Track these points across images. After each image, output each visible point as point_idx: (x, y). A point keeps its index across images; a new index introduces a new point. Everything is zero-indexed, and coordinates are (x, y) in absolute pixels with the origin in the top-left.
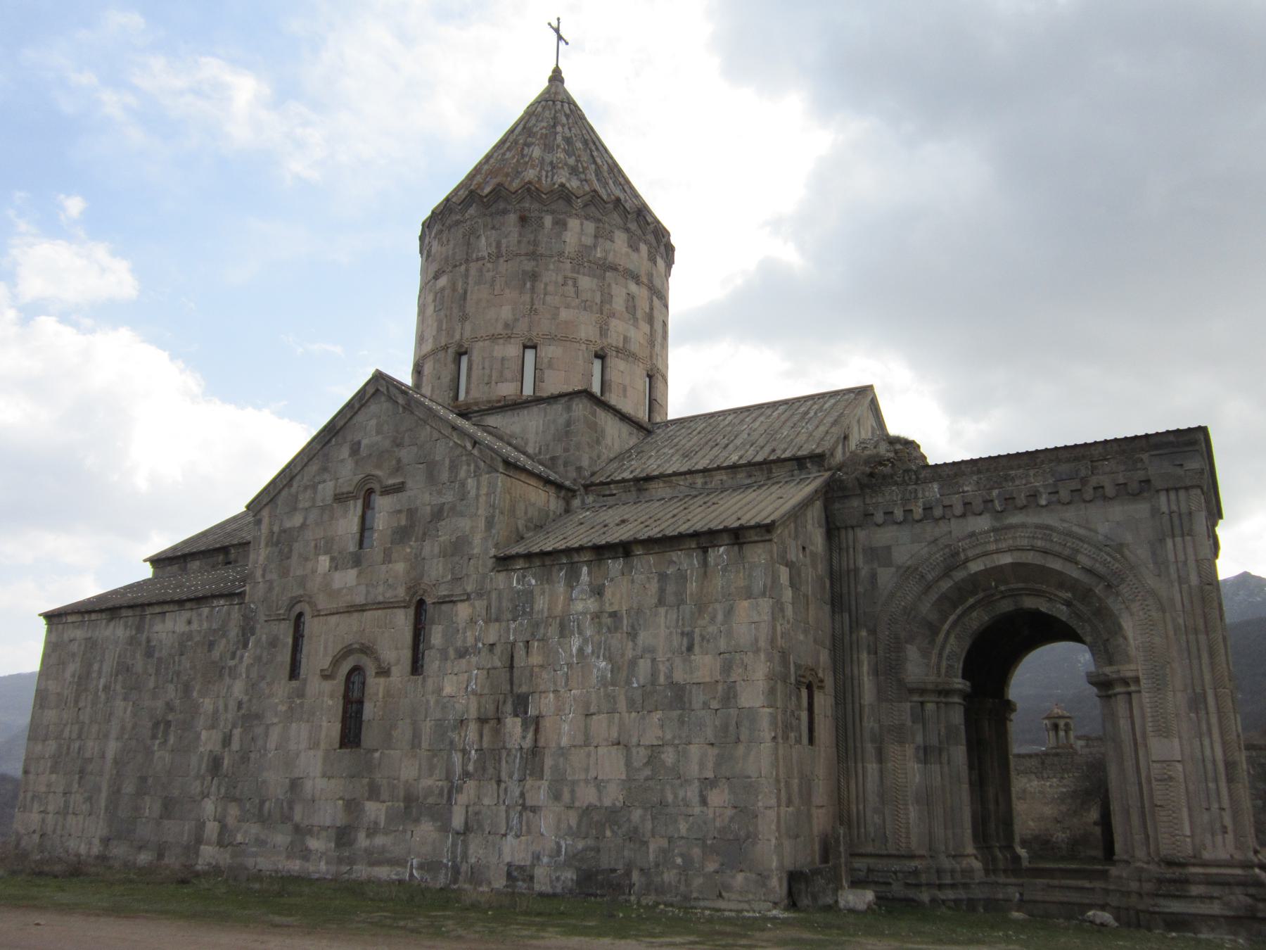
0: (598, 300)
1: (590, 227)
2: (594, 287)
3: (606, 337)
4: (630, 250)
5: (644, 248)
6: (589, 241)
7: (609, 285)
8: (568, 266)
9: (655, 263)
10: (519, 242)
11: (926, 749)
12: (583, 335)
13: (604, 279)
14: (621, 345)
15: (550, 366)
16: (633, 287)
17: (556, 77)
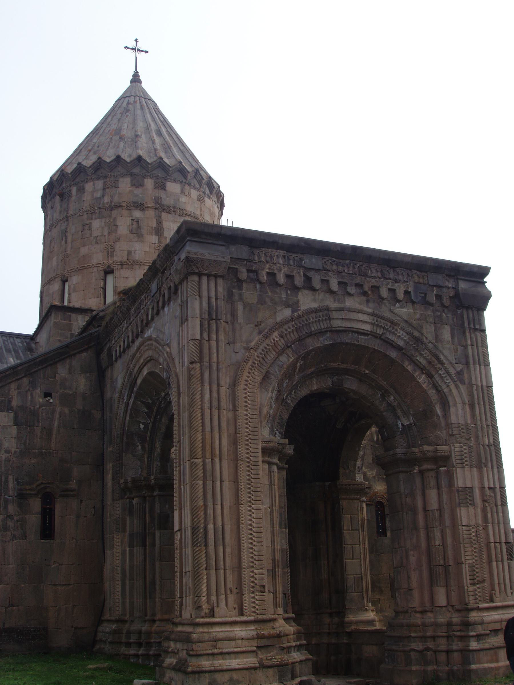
0: (106, 233)
1: (100, 184)
2: (103, 224)
3: (112, 256)
4: (133, 188)
5: (149, 183)
6: (99, 194)
7: (115, 219)
8: (85, 216)
9: (163, 187)
10: (61, 212)
11: (131, 536)
12: (94, 261)
13: (110, 216)
14: (125, 259)
15: (75, 291)
16: (137, 214)
17: (136, 79)
